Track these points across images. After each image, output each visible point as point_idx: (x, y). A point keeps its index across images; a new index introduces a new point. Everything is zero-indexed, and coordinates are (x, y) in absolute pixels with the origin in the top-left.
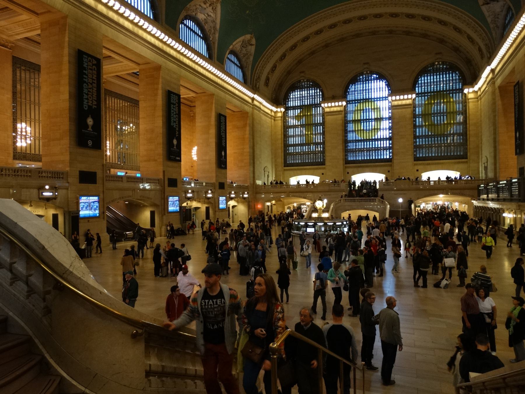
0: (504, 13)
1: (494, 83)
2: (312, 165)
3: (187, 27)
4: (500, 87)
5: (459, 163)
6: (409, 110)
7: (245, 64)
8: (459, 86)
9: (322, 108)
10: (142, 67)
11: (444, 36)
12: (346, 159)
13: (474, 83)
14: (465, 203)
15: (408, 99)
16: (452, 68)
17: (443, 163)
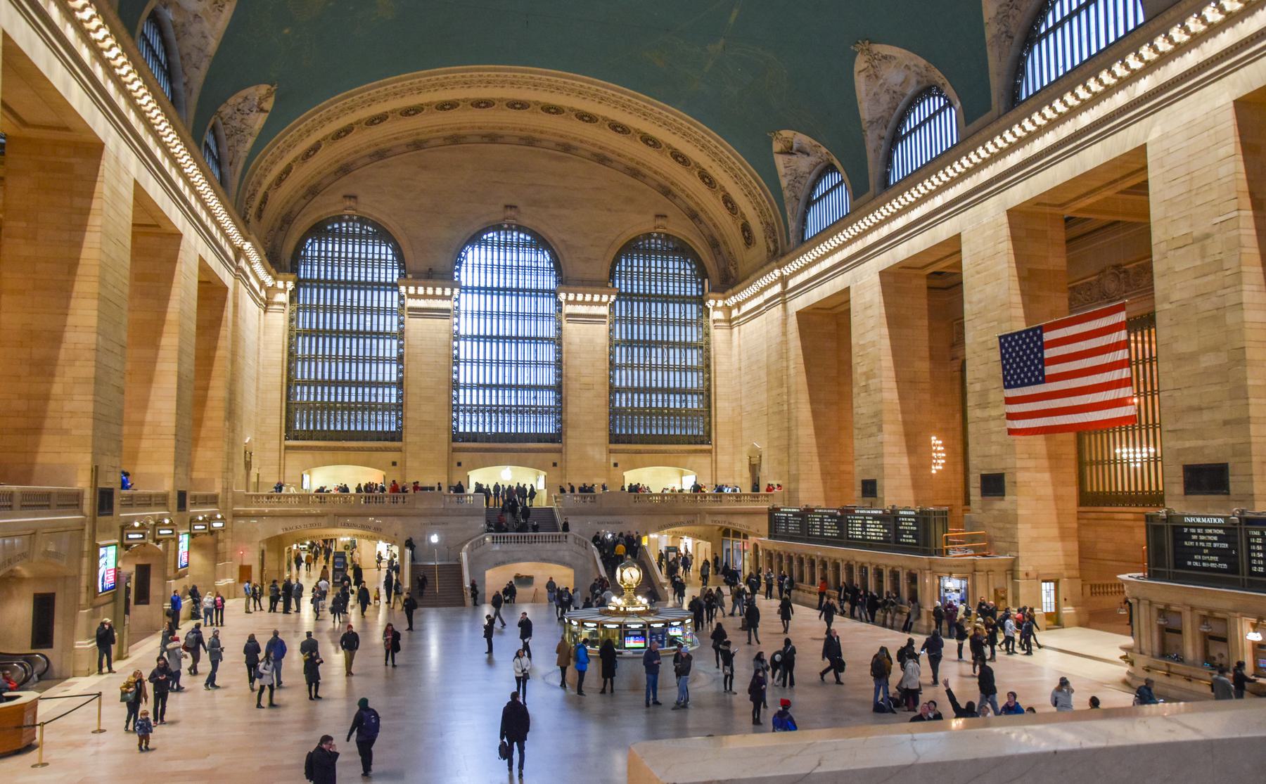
0: (812, 177)
1: (784, 303)
2: (365, 439)
4: (799, 314)
5: (696, 451)
6: (603, 329)
8: (692, 290)
10: (26, 132)
11: (672, 183)
13: (730, 291)
14: (707, 539)
15: (600, 303)
16: (682, 250)
17: (665, 452)
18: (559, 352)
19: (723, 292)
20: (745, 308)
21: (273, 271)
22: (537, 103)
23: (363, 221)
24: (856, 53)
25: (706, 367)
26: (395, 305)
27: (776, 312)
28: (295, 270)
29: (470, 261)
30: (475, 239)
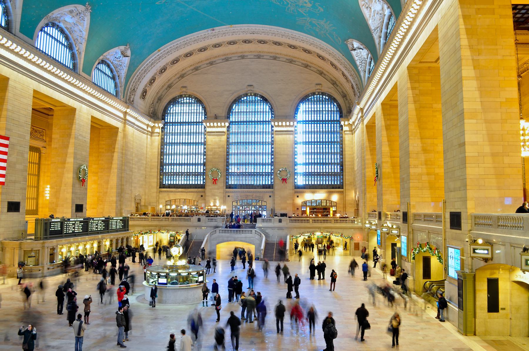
0: (369, 60)
1: (363, 121)
8: (337, 117)
12: (227, 182)
19: (348, 118)
20: (355, 124)
21: (152, 119)
22: (254, 40)
23: (190, 96)
25: (342, 153)
26: (203, 131)
27: (360, 126)
28: (163, 119)
30: (237, 100)
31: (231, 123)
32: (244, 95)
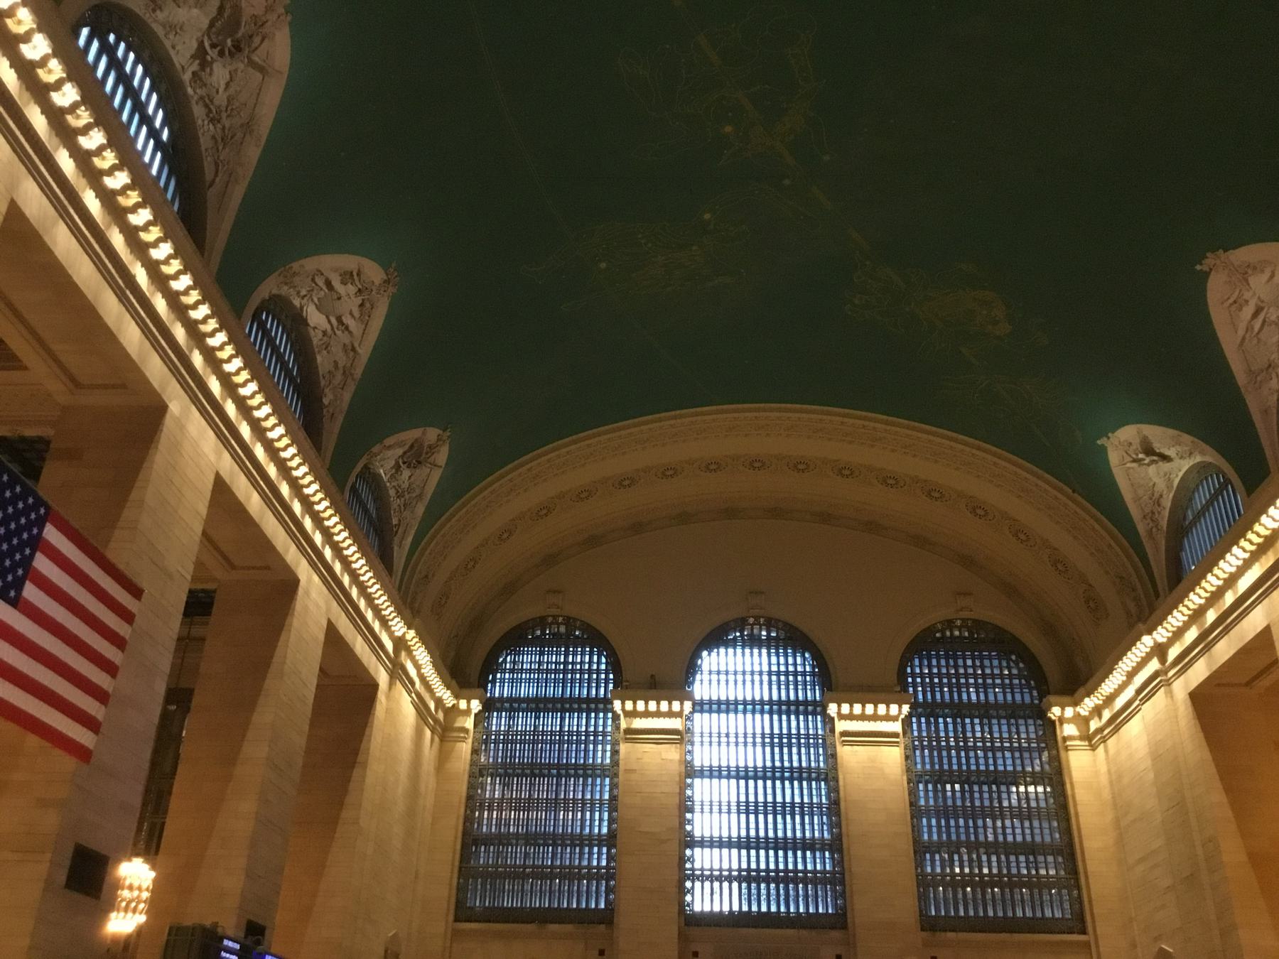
1: (1168, 683)
3: (266, 333)
7: (395, 521)
8: (1024, 697)
9: (614, 713)
13: (1082, 690)
15: (888, 718)
16: (1000, 643)
18: (834, 789)
21: (454, 682)
24: (1206, 275)
29: (705, 667)
30: (716, 639)
31: (700, 706)
32: (735, 620)
